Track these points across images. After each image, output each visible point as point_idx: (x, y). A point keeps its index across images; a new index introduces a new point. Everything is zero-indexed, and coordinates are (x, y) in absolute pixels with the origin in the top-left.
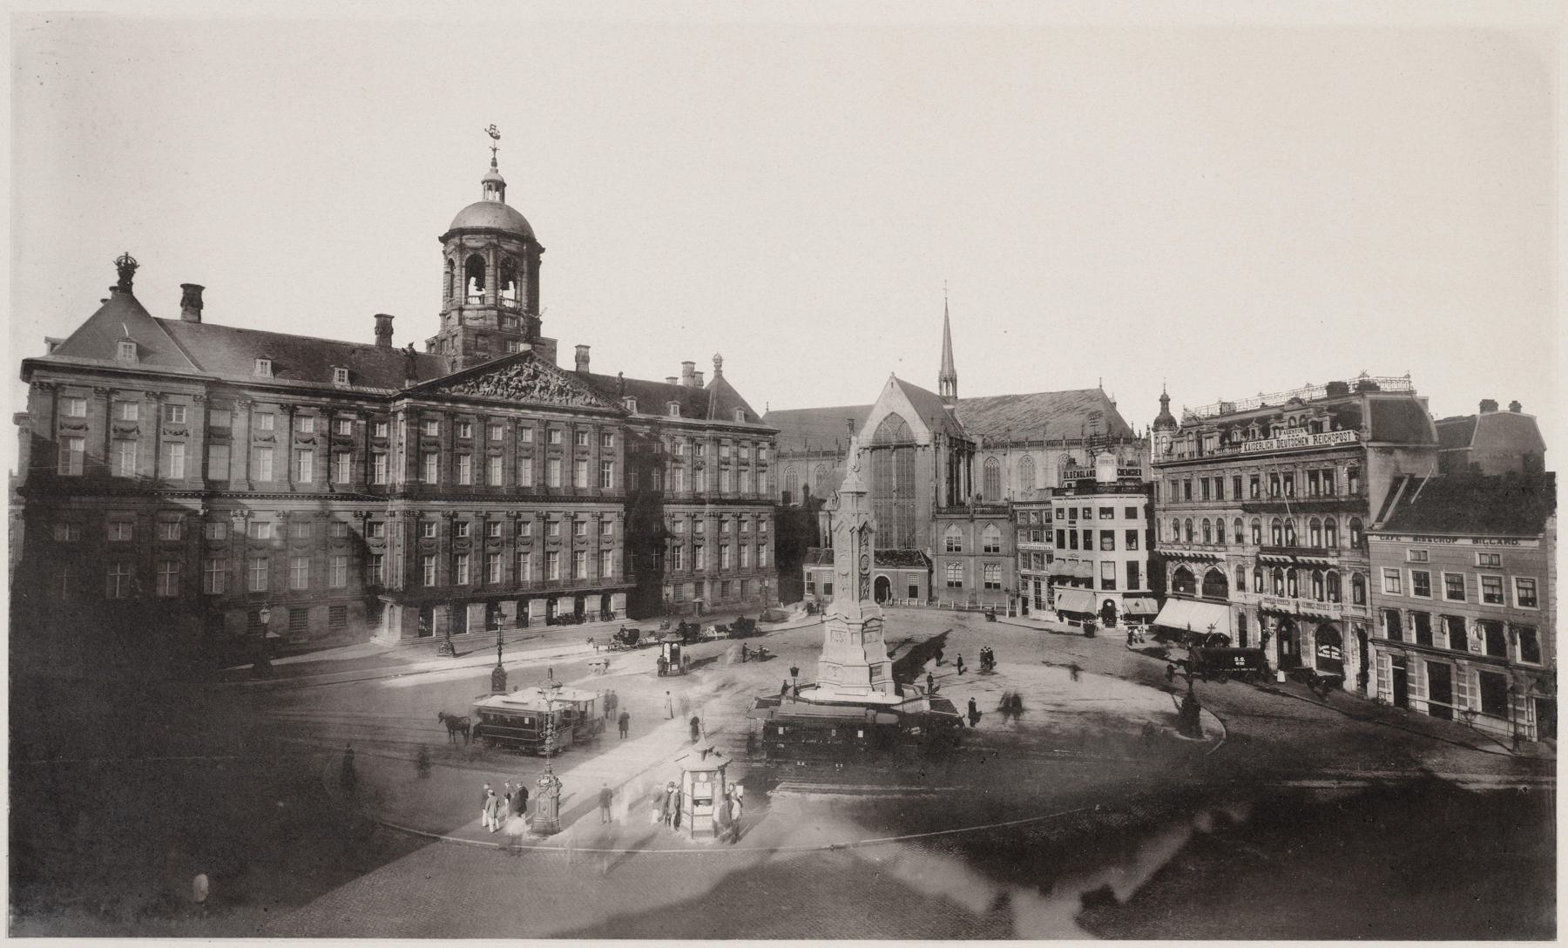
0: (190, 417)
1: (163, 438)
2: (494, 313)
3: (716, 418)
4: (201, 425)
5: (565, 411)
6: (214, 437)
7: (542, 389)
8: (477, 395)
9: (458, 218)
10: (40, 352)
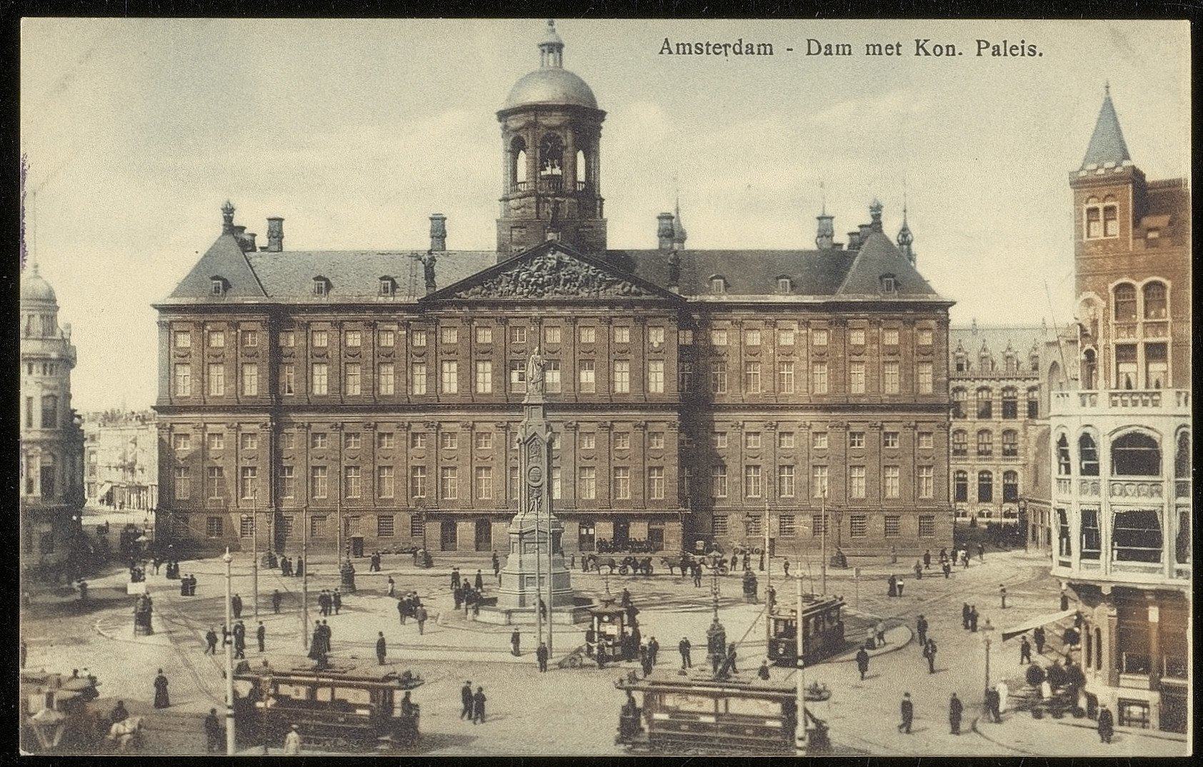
0: (258, 340)
1: (241, 360)
2: (533, 199)
3: (846, 292)
4: (267, 348)
5: (597, 304)
6: (277, 358)
7: (566, 281)
8: (495, 296)
9: (509, 99)
10: (164, 298)
